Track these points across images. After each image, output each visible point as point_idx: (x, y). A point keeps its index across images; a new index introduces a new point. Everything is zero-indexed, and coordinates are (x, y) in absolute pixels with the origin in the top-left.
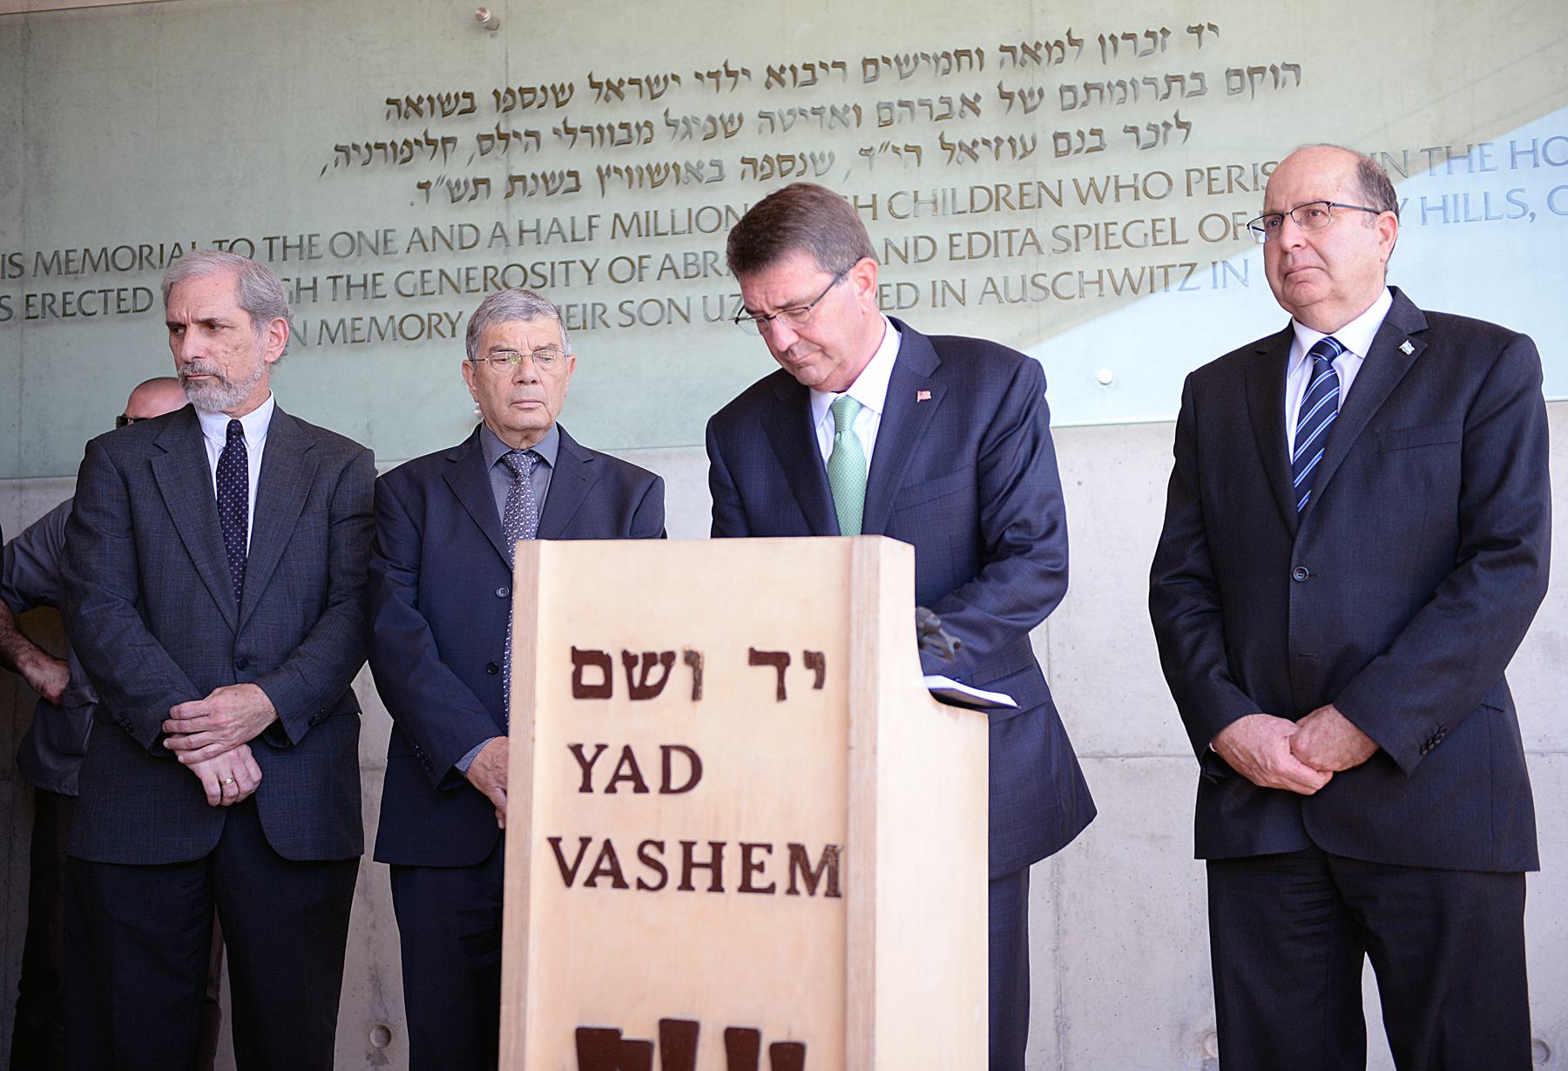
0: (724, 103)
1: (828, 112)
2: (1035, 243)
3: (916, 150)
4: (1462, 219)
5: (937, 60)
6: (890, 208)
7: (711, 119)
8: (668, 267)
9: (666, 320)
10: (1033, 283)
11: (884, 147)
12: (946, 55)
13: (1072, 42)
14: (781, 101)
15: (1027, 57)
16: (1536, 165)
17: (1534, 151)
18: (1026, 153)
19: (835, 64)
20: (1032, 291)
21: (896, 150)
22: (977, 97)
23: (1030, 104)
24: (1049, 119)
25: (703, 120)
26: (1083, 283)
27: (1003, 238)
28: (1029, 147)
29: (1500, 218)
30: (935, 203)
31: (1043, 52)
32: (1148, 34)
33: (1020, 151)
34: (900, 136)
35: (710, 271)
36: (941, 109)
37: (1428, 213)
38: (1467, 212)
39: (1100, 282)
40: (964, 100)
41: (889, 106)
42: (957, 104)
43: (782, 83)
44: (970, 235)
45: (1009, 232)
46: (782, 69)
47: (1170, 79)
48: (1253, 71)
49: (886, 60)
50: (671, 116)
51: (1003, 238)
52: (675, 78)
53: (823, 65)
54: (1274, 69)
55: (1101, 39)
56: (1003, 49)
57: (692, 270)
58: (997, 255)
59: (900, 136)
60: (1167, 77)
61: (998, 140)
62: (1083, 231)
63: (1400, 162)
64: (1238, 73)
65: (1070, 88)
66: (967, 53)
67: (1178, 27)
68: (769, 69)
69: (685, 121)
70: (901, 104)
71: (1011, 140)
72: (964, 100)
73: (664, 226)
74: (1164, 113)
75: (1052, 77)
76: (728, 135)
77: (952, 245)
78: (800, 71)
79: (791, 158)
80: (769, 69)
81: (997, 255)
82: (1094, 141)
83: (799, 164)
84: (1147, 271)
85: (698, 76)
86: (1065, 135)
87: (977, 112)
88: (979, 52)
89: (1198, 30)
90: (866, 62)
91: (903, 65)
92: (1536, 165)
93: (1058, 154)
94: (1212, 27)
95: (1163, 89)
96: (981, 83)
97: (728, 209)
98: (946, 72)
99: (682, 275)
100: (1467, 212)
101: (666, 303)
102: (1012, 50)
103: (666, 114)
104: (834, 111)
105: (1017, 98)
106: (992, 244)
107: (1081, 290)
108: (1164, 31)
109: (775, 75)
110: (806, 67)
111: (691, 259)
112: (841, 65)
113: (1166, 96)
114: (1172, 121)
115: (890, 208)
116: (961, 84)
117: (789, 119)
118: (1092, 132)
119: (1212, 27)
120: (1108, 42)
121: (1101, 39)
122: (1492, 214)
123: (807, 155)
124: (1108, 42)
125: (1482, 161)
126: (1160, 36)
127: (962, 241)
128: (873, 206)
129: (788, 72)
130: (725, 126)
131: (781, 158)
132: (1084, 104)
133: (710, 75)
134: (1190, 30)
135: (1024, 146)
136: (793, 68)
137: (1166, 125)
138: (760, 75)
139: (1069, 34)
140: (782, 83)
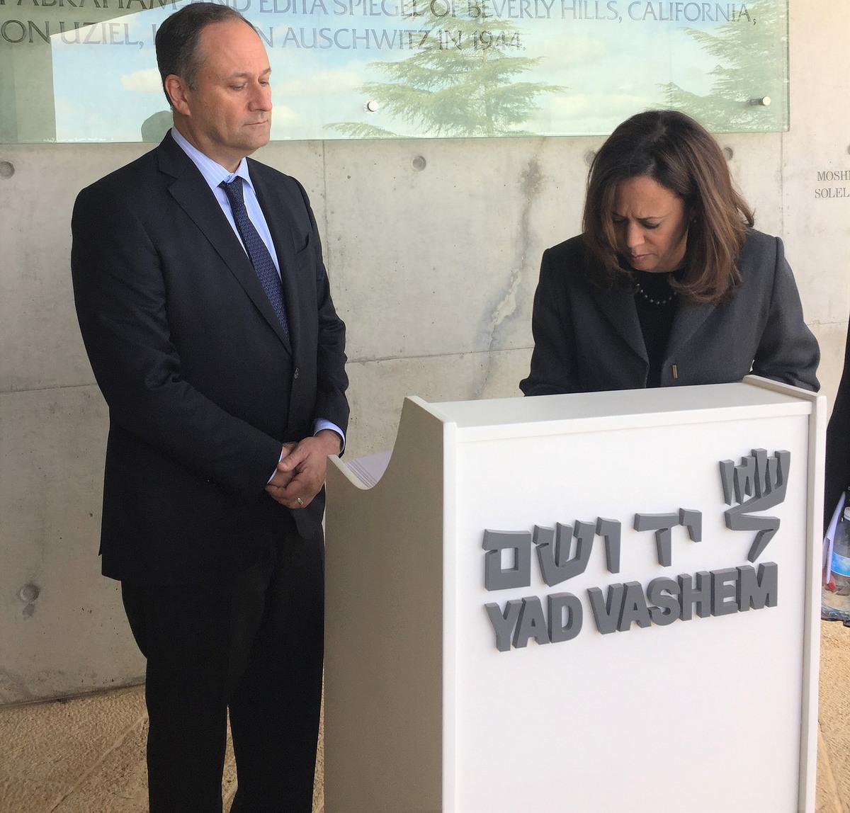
2: (322, 5)
4: (583, 17)
29: (604, 18)
37: (565, 11)
38: (586, 14)
39: (367, 38)
58: (294, 12)
81: (294, 12)
84: (398, 33)
100: (586, 14)
107: (354, 42)
122: (600, 16)
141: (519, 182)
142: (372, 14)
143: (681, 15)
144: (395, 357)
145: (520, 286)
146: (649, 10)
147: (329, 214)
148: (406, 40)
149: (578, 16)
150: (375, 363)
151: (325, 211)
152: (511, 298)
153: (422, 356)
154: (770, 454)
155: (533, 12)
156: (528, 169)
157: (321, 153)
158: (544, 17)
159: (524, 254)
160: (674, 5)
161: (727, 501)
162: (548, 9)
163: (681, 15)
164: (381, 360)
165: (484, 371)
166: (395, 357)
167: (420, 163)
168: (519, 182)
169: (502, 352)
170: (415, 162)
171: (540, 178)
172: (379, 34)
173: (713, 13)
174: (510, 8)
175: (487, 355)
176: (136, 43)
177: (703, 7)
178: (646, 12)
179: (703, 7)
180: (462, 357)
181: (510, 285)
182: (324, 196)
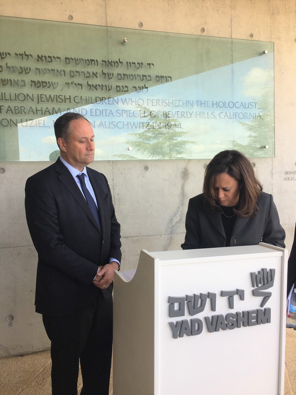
0: (25, 64)
1: (56, 71)
2: (112, 113)
3: (81, 85)
5: (86, 62)
6: (74, 100)
7: (21, 68)
8: (9, 110)
9: (9, 125)
10: (112, 124)
11: (72, 83)
12: (88, 60)
13: (121, 62)
14: (41, 66)
15: (109, 64)
16: (217, 107)
17: (216, 104)
18: (109, 90)
19: (58, 58)
20: (111, 125)
21: (76, 84)
22: (97, 73)
23: (110, 77)
24: (114, 83)
25: (18, 67)
26: (124, 125)
27: (104, 111)
28: (110, 88)
29: (210, 118)
30: (86, 100)
31: (113, 64)
32: (138, 63)
33: (108, 89)
34: (77, 80)
35: (23, 112)
36: (87, 75)
37: (197, 115)
39: (128, 125)
40: (93, 73)
41: (73, 72)
42: (91, 73)
43: (42, 60)
44: (96, 110)
45: (106, 110)
46: (42, 56)
47: (144, 76)
48: (162, 77)
49: (72, 59)
50: (8, 65)
51: (104, 111)
52: (9, 54)
53: (54, 57)
54: (166, 77)
55: (127, 62)
56: (103, 61)
57: (17, 112)
58: (103, 116)
59: (77, 80)
60: (143, 75)
61: (102, 85)
62: (124, 112)
63: (191, 103)
64: (158, 77)
65: (120, 74)
66: (93, 60)
67: (145, 63)
68: (38, 56)
69: (13, 67)
70: (77, 72)
71: (105, 86)
72: (93, 73)
73: (8, 98)
74: (142, 84)
75: (116, 71)
76: (26, 73)
77: (91, 112)
78: (47, 58)
79: (46, 82)
80: (38, 56)
81: (103, 116)
82: (126, 89)
83: (48, 85)
84: (139, 123)
85: (16, 54)
86: (119, 86)
87: (97, 77)
88: (97, 60)
89: (149, 64)
90: (66, 58)
91: (77, 61)
92: (217, 107)
93: (117, 91)
94: (153, 64)
95: (142, 78)
96: (98, 69)
97: (27, 95)
98: (88, 65)
99: (14, 112)
101: (9, 120)
102: (105, 61)
103: (7, 64)
104: (57, 71)
105: (107, 74)
106: (101, 112)
107: (123, 126)
108: (142, 63)
109: (40, 58)
110: (49, 57)
111: (17, 108)
112: (59, 58)
113: (143, 80)
114: (144, 86)
115: (74, 100)
116: (91, 69)
117: (44, 71)
118: (126, 87)
119: (153, 64)
120: (129, 64)
121: (127, 62)
122: (209, 117)
123: (50, 82)
124: (129, 64)
125: (207, 105)
126: (141, 64)
127: (94, 111)
128: (70, 99)
129: (44, 57)
130: (25, 70)
131: (43, 82)
132: (123, 79)
133: (20, 54)
134: (148, 64)
135: (109, 88)
136: (45, 57)
137: (142, 87)
138: (35, 56)
139: (119, 60)
140: (42, 60)
141: (181, 175)
142: (129, 116)
143: (237, 117)
144: (138, 236)
145: (181, 211)
146: (226, 115)
147: (114, 186)
148: (141, 125)
149: (201, 117)
150: (130, 238)
151: (113, 185)
152: (178, 216)
153: (147, 236)
154: (268, 270)
155: (186, 116)
156: (184, 170)
157: (112, 165)
158: (189, 117)
159: (183, 200)
160: (235, 113)
161: (253, 286)
162: (191, 115)
163: (237, 117)
164: (133, 237)
165: (169, 241)
166: (138, 236)
167: (146, 168)
168: (181, 175)
169: (175, 234)
170: (145, 168)
171: (188, 174)
172: (132, 123)
173: (248, 116)
174: (178, 114)
175: (170, 235)
176: (47, 127)
177: (245, 114)
178: (225, 116)
179: (245, 114)
180: (161, 236)
181: (178, 211)
182: (113, 180)
